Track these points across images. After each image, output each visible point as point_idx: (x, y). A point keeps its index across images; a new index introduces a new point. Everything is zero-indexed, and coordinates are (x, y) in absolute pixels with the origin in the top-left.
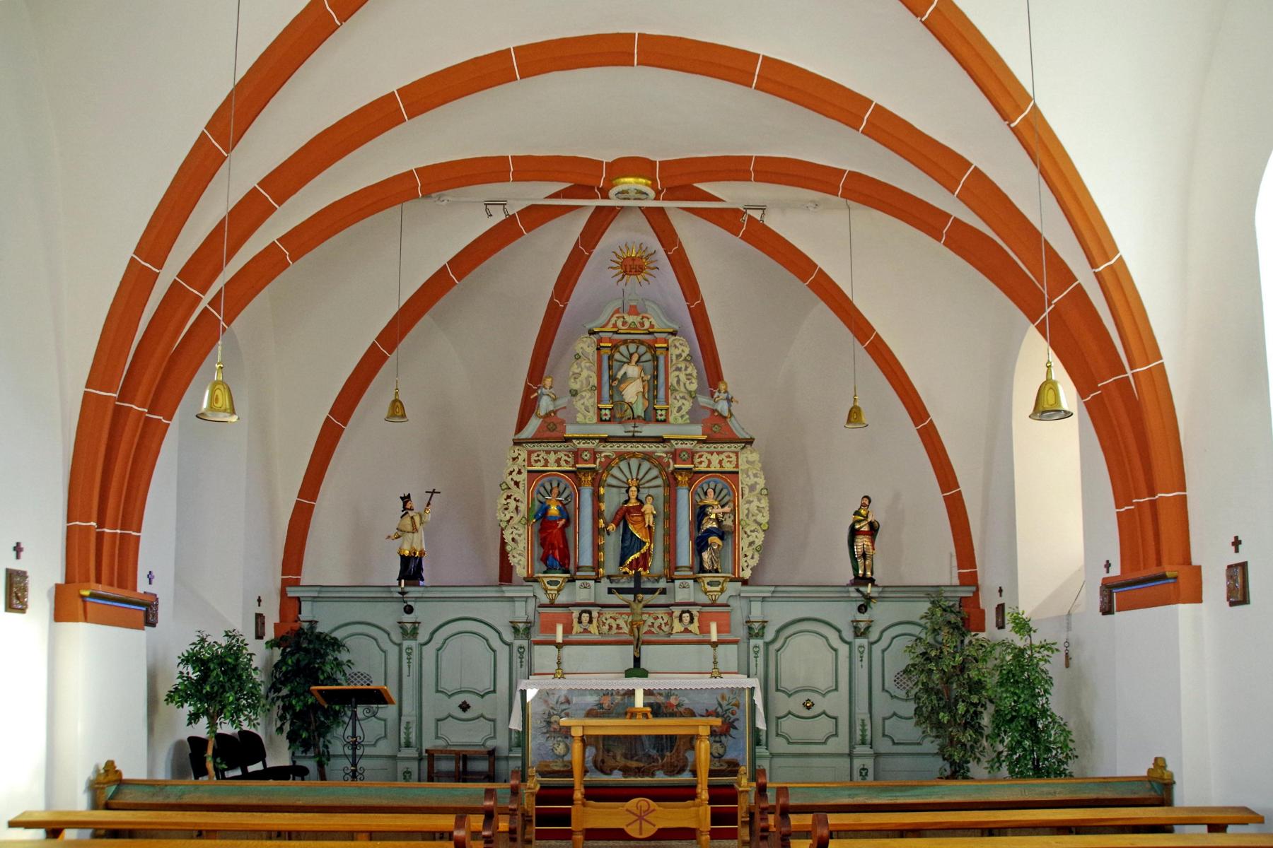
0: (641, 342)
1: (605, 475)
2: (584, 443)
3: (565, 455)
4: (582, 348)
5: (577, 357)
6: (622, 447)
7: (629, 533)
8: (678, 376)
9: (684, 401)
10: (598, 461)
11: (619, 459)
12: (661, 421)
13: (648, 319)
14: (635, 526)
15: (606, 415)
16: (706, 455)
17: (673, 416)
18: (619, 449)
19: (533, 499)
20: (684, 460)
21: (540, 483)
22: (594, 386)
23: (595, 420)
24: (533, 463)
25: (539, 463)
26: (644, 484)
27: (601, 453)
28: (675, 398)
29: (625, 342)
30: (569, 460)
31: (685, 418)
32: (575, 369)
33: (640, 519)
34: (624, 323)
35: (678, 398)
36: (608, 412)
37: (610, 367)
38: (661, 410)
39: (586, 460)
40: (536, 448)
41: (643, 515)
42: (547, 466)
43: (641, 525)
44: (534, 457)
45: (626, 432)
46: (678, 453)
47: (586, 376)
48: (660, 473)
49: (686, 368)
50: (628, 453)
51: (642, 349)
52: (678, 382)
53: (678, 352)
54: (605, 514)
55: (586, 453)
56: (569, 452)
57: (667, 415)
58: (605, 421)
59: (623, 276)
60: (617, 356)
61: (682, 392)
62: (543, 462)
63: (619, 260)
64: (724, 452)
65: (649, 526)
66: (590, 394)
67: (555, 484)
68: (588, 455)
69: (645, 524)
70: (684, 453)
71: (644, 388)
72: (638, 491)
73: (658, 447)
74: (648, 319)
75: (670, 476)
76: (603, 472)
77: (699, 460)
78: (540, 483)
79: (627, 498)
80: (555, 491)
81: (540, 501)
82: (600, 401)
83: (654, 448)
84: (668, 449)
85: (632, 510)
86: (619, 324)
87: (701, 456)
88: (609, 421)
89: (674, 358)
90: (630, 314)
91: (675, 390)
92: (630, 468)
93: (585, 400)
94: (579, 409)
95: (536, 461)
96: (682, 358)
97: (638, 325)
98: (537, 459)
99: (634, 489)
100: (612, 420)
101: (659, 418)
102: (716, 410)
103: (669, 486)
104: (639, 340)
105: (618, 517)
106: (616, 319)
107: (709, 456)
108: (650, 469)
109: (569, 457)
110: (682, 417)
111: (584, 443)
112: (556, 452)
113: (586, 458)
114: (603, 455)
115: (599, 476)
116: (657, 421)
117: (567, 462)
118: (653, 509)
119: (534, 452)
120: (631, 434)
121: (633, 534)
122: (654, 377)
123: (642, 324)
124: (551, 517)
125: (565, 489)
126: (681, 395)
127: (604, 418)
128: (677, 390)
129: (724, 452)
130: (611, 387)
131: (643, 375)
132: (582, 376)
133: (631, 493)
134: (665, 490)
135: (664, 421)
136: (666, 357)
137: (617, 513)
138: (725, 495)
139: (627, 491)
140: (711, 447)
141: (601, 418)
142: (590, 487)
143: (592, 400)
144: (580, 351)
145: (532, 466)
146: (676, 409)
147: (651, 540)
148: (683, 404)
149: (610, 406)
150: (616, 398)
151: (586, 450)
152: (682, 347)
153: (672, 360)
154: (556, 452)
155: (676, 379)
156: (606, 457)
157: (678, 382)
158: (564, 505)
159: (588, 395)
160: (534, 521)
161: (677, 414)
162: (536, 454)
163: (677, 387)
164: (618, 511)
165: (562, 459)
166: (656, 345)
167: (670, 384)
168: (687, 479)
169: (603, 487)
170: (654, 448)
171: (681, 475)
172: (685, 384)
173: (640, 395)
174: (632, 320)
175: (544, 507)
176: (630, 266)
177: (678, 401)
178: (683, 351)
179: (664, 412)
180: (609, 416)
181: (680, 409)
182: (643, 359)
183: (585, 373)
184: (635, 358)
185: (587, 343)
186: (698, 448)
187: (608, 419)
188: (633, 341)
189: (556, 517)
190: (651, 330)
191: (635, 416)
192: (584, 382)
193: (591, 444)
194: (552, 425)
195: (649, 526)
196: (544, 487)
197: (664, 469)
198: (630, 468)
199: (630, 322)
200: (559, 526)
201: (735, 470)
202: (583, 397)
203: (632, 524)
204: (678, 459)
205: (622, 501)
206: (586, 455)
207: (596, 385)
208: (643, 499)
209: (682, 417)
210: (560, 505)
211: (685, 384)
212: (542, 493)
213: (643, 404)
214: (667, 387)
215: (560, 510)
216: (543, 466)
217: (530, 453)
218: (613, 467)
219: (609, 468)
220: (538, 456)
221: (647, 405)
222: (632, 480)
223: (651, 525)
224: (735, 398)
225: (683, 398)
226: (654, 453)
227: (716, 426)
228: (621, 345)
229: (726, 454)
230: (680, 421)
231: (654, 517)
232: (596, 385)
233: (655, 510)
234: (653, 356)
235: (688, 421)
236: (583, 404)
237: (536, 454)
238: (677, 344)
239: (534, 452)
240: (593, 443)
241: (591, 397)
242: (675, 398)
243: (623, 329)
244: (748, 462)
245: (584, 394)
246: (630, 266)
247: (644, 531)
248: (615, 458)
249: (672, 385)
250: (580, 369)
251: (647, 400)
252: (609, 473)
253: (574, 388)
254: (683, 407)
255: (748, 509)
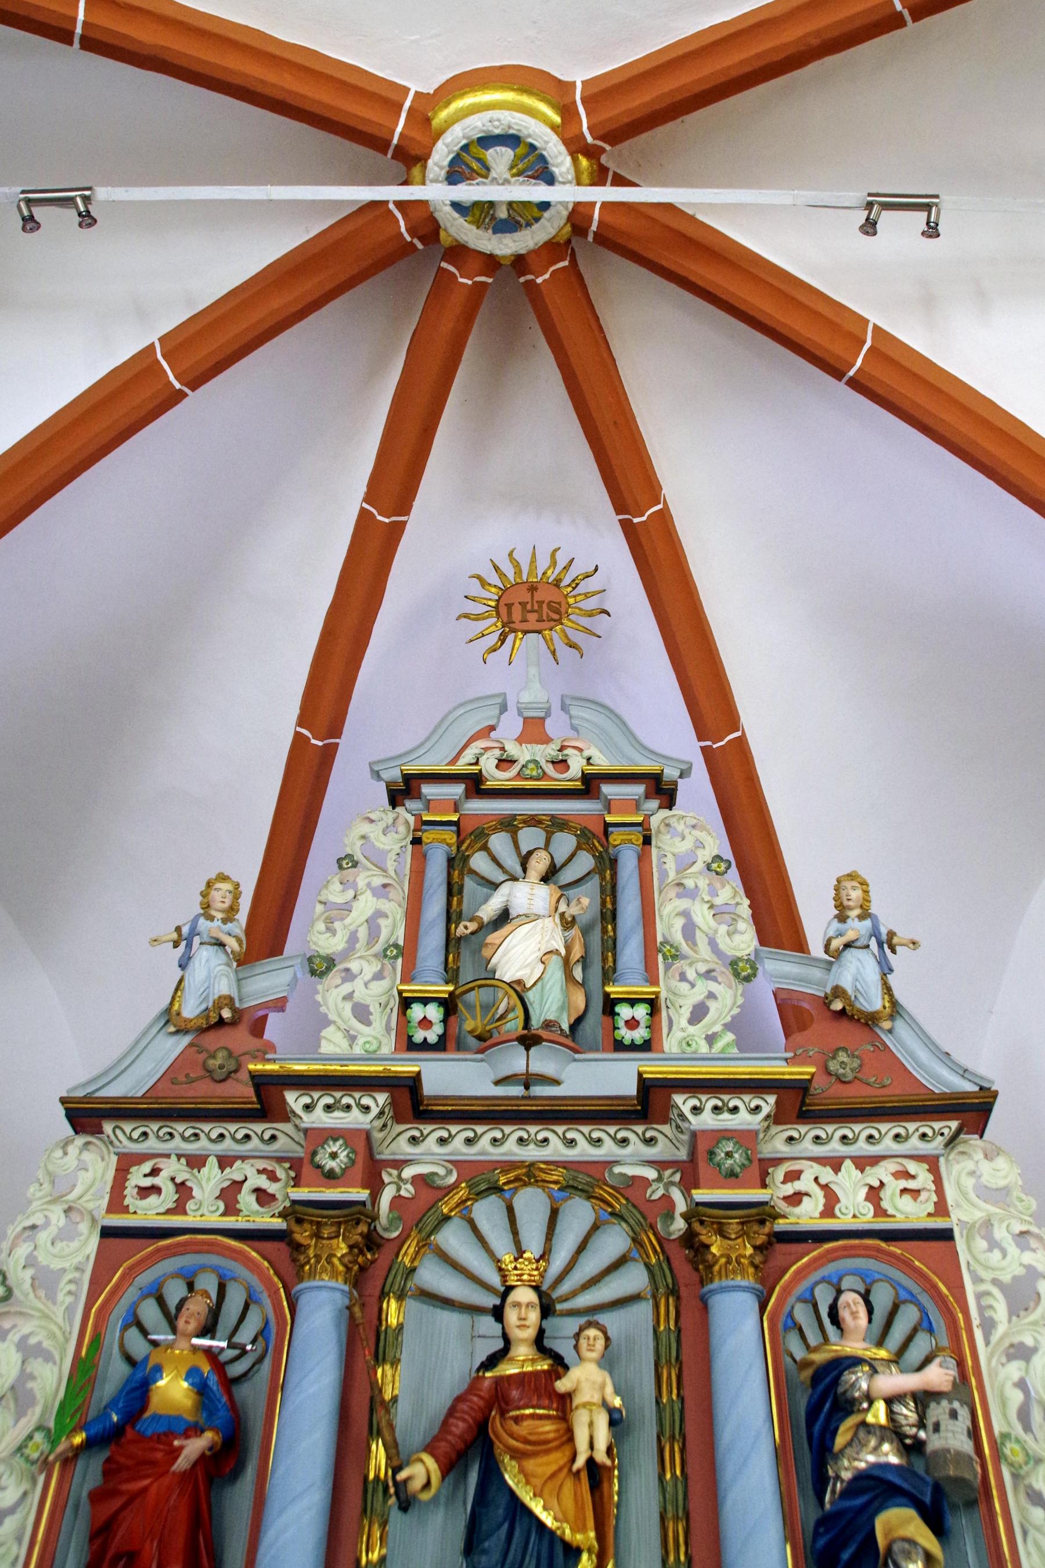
0: (557, 824)
1: (410, 1248)
2: (328, 1108)
3: (259, 1172)
4: (363, 837)
5: (347, 862)
6: (485, 1142)
7: (503, 1501)
8: (686, 914)
9: (713, 986)
10: (387, 1195)
11: (470, 1187)
12: (633, 1047)
13: (581, 750)
14: (530, 1464)
15: (425, 1023)
16: (811, 1171)
17: (677, 1035)
18: (470, 1153)
19: (97, 1339)
20: (732, 1174)
21: (146, 1278)
22: (396, 946)
23: (388, 1047)
24: (130, 1198)
25: (153, 1199)
26: (574, 1294)
27: (399, 1164)
28: (683, 977)
29: (509, 825)
30: (272, 1188)
31: (719, 1045)
32: (335, 894)
33: (548, 1428)
34: (505, 762)
35: (691, 974)
36: (434, 1012)
37: (453, 890)
38: (633, 1002)
39: (330, 1176)
40: (152, 1144)
41: (564, 1402)
42: (185, 1213)
43: (557, 1459)
44: (138, 1177)
45: (497, 1083)
46: (702, 1147)
47: (369, 913)
48: (634, 1240)
49: (714, 893)
50: (508, 1166)
51: (565, 843)
52: (690, 930)
53: (683, 847)
54: (402, 1415)
55: (334, 1147)
56: (280, 1160)
57: (653, 1026)
58: (425, 1046)
59: (503, 639)
60: (479, 862)
61: (705, 961)
62: (169, 1195)
63: (485, 594)
64: (884, 1157)
65: (591, 1462)
66: (376, 966)
67: (208, 1283)
68: (343, 1155)
69: (573, 1459)
70: (729, 1146)
71: (568, 948)
72: (547, 1310)
73: (625, 1141)
74: (581, 750)
75: (680, 1256)
76: (402, 1240)
77: (789, 1189)
78: (146, 1278)
79: (500, 1344)
80: (197, 1308)
81: (129, 1359)
82: (406, 978)
83: (608, 1142)
84: (660, 1151)
85: (515, 1394)
86: (488, 765)
87: (793, 1176)
88: (441, 1045)
89: (671, 866)
90: (521, 740)
91: (677, 956)
92: (515, 1232)
93: (358, 985)
94: (332, 1016)
95: (145, 1192)
96: (699, 866)
97: (550, 769)
98: (147, 1182)
99: (524, 1295)
100: (451, 1044)
101: (626, 1035)
102: (838, 992)
103: (674, 1291)
104: (553, 817)
105: (459, 1427)
106: (478, 751)
107: (826, 1175)
108: (595, 1228)
109: (273, 1177)
110: (711, 1039)
111: (328, 1108)
112: (225, 1162)
113: (330, 1164)
114: (408, 1172)
115: (383, 1258)
116: (619, 1046)
117: (263, 1197)
118: (609, 1389)
119: (140, 1158)
120: (517, 1091)
121: (518, 1509)
122: (603, 915)
123: (561, 764)
124: (157, 1418)
125: (246, 1307)
126: (702, 968)
127: (419, 1036)
128: (685, 957)
129: (884, 1157)
130: (452, 943)
131: (563, 907)
132: (354, 914)
133: (511, 1316)
134: (656, 1306)
135: (646, 1046)
136: (643, 858)
137: (452, 1412)
138: (915, 1331)
139: (498, 1313)
140: (830, 1139)
141: (410, 1037)
142: (340, 1284)
143: (385, 984)
144: (356, 849)
145: (125, 1210)
146: (686, 1013)
147: (601, 1537)
148: (711, 996)
149: (444, 989)
150: (467, 974)
151: (334, 1134)
152: (696, 833)
153: (664, 874)
154: (225, 1162)
155: (679, 923)
156: (420, 1180)
157: (690, 930)
158: (229, 1383)
159: (370, 969)
160: (78, 1439)
161: (692, 1029)
162: (147, 1167)
163: (685, 948)
164: (459, 1399)
165: (247, 1187)
166: (609, 819)
167: (659, 939)
168: (749, 1251)
169: (400, 1298)
170: (608, 1149)
171: (722, 1233)
172: (713, 943)
173: (556, 963)
174: (528, 758)
175: (139, 1375)
176: (523, 604)
177: (693, 986)
178: (700, 845)
179: (641, 1012)
180: (438, 1029)
181: (698, 1013)
182: (567, 876)
183: (366, 905)
184: (539, 864)
185: (382, 825)
186: (776, 1144)
187: (432, 1037)
188: (533, 821)
189: (178, 1418)
190: (590, 770)
191: (536, 1022)
192: (363, 933)
193: (355, 1111)
194: (221, 1055)
195: (591, 1462)
196: (161, 1301)
197: (652, 1227)
198: (515, 1232)
199: (522, 761)
200: (182, 1463)
201: (939, 1223)
202: (349, 976)
203: (517, 1455)
204: (704, 1169)
205: (481, 1357)
206: (334, 1156)
207: (401, 943)
208: (564, 1349)
209: (711, 1039)
210: (206, 1368)
211: (713, 943)
212: (148, 1323)
213: (567, 994)
214: (651, 948)
215: (201, 1389)
216: (169, 1212)
217: (126, 1163)
218: (447, 1218)
219: (431, 1220)
220: (155, 1172)
221: (582, 1006)
222: (520, 1253)
223: (601, 1457)
224: (903, 934)
225: (708, 975)
226: (610, 1164)
227: (842, 1057)
228: (496, 830)
229: (890, 1166)
230: (704, 1048)
231: (612, 1423)
232: (401, 943)
233: (617, 1392)
234: (599, 858)
235: (734, 1051)
236: (348, 997)
237: (147, 1167)
238: (680, 827)
239: (140, 1158)
240: (367, 1109)
241: (378, 976)
242: (683, 977)
243: (497, 778)
244: (987, 1193)
245: (354, 966)
246: (523, 604)
247: (569, 1486)
248: (455, 1186)
249: (665, 942)
250: (351, 893)
251: (583, 985)
252: (425, 1244)
253: (323, 952)
254: (712, 1005)
255: (1022, 1385)
